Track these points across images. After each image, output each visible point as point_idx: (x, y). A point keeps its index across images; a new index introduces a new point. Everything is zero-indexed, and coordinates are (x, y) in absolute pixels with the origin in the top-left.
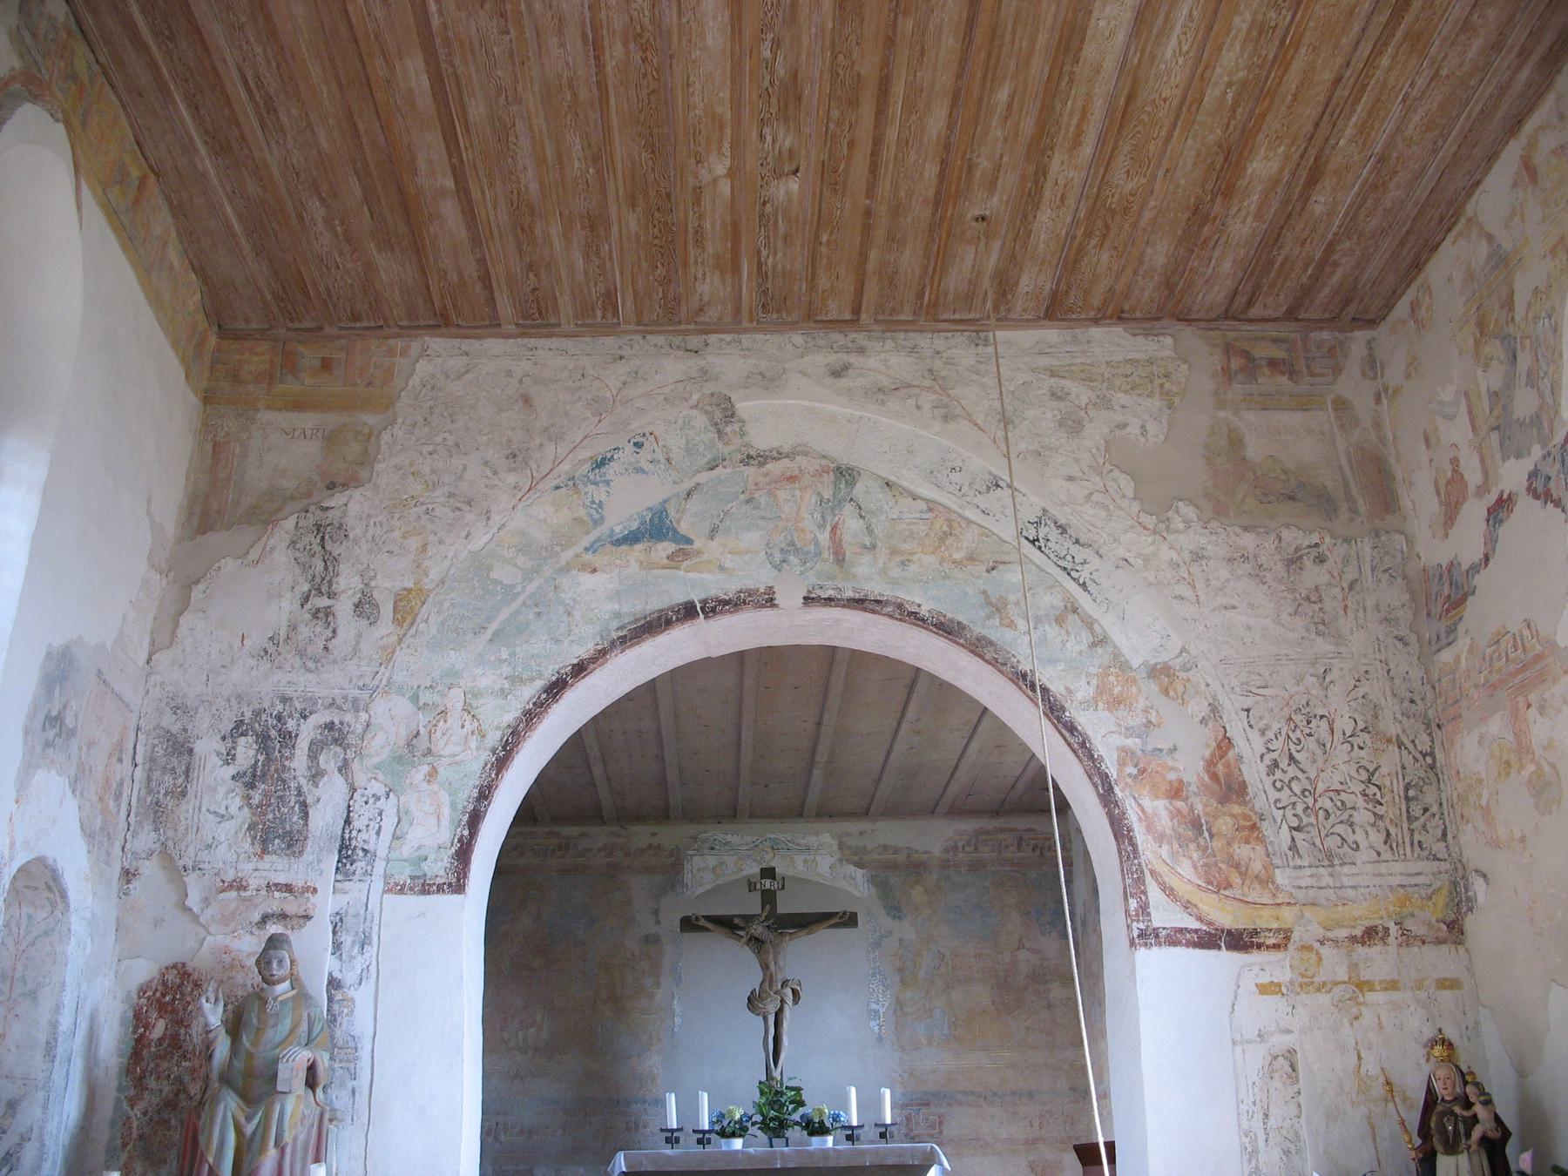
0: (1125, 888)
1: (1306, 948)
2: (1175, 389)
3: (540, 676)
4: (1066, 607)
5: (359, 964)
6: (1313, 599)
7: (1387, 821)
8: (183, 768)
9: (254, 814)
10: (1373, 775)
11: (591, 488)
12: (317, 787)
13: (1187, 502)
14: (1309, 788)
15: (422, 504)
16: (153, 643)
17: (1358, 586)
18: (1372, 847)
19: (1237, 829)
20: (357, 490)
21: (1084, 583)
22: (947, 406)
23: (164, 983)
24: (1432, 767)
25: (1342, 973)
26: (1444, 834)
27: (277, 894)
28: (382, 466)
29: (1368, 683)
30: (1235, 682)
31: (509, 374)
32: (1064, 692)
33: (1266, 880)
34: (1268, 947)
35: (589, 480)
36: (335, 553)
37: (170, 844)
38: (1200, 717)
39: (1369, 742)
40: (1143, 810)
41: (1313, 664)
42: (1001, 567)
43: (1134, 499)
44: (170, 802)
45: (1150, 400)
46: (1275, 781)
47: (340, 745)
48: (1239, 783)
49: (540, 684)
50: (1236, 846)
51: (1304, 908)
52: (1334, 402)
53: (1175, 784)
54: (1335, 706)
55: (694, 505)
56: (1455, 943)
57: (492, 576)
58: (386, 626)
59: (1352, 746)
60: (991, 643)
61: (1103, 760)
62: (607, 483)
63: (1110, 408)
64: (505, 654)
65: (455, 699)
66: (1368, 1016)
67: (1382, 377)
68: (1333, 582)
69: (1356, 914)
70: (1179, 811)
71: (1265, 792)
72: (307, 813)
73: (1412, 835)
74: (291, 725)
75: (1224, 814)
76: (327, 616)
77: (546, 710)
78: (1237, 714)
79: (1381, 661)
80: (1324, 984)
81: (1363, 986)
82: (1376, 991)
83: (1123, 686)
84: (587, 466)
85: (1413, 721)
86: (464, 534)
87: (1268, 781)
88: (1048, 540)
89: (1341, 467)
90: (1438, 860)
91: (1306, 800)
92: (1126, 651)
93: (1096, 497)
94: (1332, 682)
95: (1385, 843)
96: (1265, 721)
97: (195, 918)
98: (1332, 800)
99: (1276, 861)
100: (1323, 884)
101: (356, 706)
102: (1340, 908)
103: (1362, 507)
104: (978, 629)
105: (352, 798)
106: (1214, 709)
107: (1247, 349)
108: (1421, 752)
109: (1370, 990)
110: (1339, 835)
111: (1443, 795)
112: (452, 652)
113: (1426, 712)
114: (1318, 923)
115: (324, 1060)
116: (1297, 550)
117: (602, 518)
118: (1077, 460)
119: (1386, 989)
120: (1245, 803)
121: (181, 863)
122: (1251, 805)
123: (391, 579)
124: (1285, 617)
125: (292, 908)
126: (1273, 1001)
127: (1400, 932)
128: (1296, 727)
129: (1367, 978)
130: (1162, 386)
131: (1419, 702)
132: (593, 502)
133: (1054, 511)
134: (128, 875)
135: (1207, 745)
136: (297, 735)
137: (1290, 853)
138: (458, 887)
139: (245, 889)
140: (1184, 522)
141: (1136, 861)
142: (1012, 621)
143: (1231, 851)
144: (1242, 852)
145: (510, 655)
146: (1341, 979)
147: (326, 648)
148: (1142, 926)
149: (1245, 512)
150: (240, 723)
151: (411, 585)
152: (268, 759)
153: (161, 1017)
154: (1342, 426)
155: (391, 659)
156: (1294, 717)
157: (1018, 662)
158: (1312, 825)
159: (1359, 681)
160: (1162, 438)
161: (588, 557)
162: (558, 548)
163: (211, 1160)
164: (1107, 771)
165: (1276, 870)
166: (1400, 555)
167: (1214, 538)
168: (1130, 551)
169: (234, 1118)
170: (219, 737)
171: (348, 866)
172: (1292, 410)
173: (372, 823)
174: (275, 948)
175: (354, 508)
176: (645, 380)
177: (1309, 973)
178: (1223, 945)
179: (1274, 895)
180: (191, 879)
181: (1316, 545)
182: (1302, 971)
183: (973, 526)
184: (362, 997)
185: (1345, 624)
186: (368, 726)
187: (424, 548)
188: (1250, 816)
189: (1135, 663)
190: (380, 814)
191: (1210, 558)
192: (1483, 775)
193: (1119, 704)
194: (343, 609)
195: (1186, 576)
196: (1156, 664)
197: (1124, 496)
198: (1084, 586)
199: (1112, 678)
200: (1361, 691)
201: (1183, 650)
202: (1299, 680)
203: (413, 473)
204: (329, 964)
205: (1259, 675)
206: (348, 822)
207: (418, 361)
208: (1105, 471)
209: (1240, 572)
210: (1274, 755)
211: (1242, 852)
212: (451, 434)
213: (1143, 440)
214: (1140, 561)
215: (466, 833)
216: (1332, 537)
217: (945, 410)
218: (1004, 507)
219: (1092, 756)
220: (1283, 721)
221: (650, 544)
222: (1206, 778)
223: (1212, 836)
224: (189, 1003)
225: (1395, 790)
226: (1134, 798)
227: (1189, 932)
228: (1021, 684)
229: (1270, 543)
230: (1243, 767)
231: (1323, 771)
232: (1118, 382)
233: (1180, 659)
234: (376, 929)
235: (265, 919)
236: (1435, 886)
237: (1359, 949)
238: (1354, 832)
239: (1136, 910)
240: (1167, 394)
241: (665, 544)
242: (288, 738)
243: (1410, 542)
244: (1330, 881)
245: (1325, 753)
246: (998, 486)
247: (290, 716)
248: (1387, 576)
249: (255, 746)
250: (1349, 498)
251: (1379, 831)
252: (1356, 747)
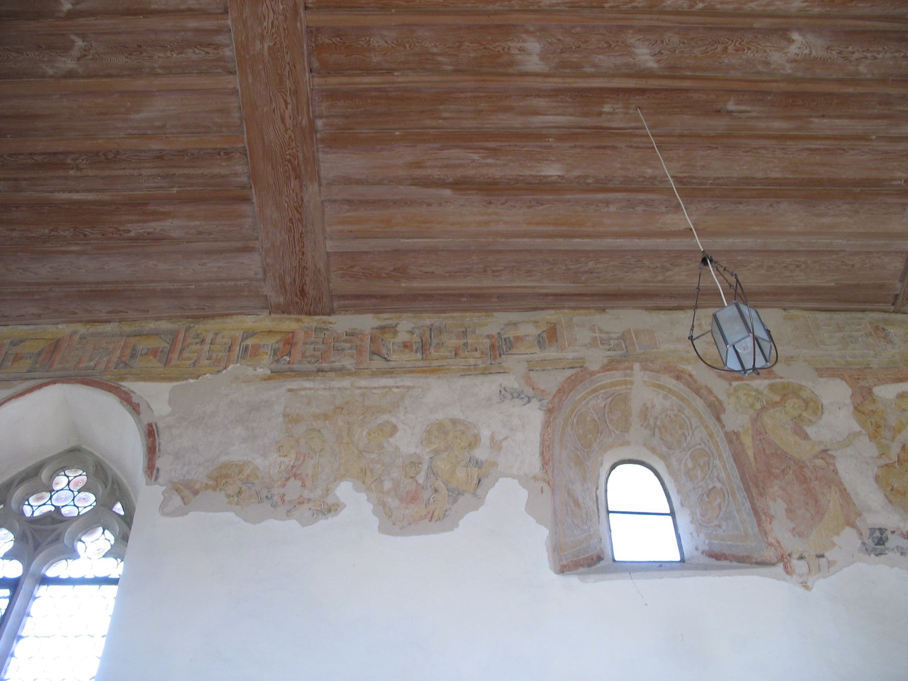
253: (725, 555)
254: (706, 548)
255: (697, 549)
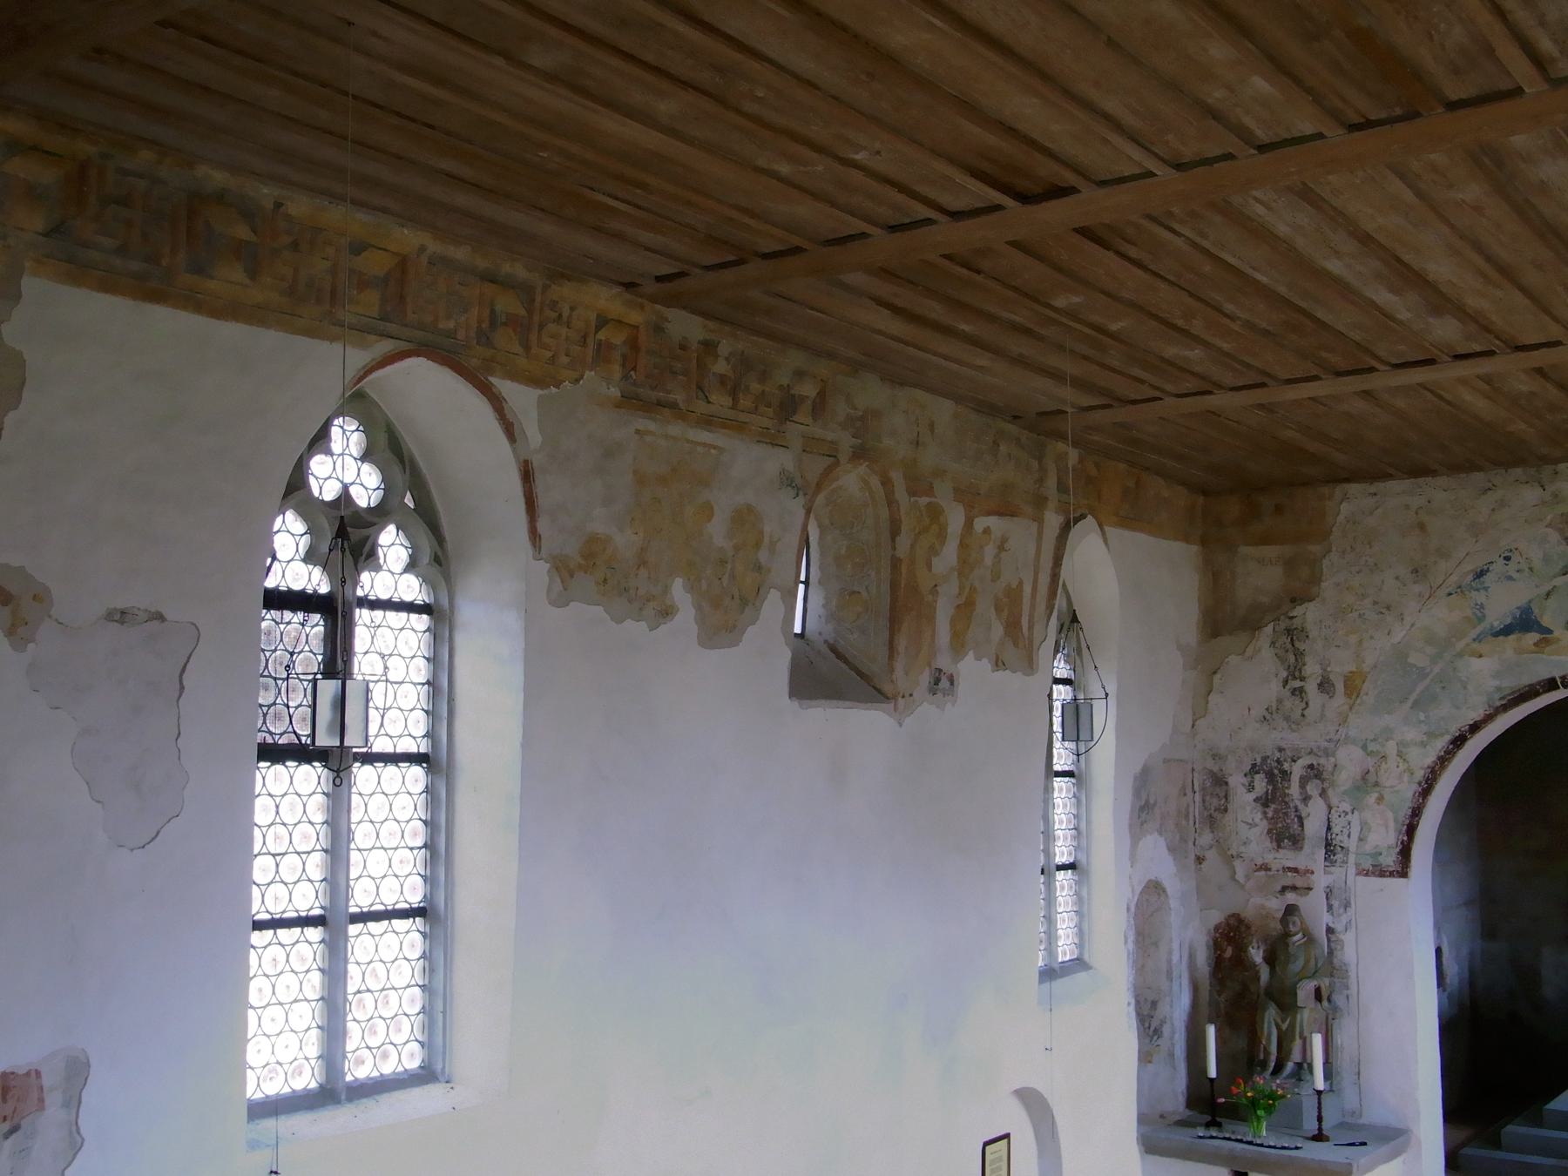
3: (1447, 732)
5: (1344, 919)
8: (1224, 794)
9: (1269, 824)
11: (1474, 593)
12: (1307, 806)
15: (1356, 610)
16: (1194, 714)
20: (1310, 603)
23: (1228, 924)
27: (1289, 874)
28: (1327, 584)
31: (1407, 507)
35: (1472, 588)
36: (1302, 648)
37: (1221, 840)
44: (1217, 815)
47: (1320, 779)
49: (1448, 738)
55: (1552, 603)
57: (1409, 660)
58: (1340, 699)
62: (1486, 589)
64: (1422, 716)
65: (1391, 748)
72: (1303, 824)
74: (1286, 766)
76: (1301, 693)
77: (1453, 756)
84: (1470, 577)
86: (1386, 632)
97: (1242, 887)
101: (1327, 753)
105: (1330, 813)
112: (1386, 716)
115: (1325, 983)
117: (1484, 616)
121: (1229, 853)
123: (1341, 665)
125: (1299, 884)
132: (1477, 604)
134: (1200, 860)
136: (1291, 773)
138: (1403, 873)
139: (1270, 870)
145: (1425, 717)
147: (1303, 715)
150: (1254, 766)
151: (1354, 669)
152: (1275, 789)
153: (1229, 945)
155: (1346, 721)
161: (1475, 645)
162: (1454, 640)
163: (1264, 1042)
169: (1275, 1020)
170: (1242, 775)
171: (1332, 857)
173: (1345, 830)
174: (1290, 915)
175: (1310, 617)
176: (1509, 506)
180: (1237, 863)
184: (1348, 938)
186: (1336, 766)
187: (1360, 642)
190: (1349, 824)
194: (1311, 687)
203: (1347, 589)
204: (1326, 919)
206: (1329, 828)
207: (1341, 503)
212: (1371, 557)
215: (1405, 838)
221: (1519, 635)
224: (1244, 938)
234: (1352, 897)
235: (1284, 889)
241: (1533, 634)
242: (1286, 775)
247: (1285, 760)
249: (1266, 780)
253: (846, 658)
254: (831, 641)
255: (820, 634)
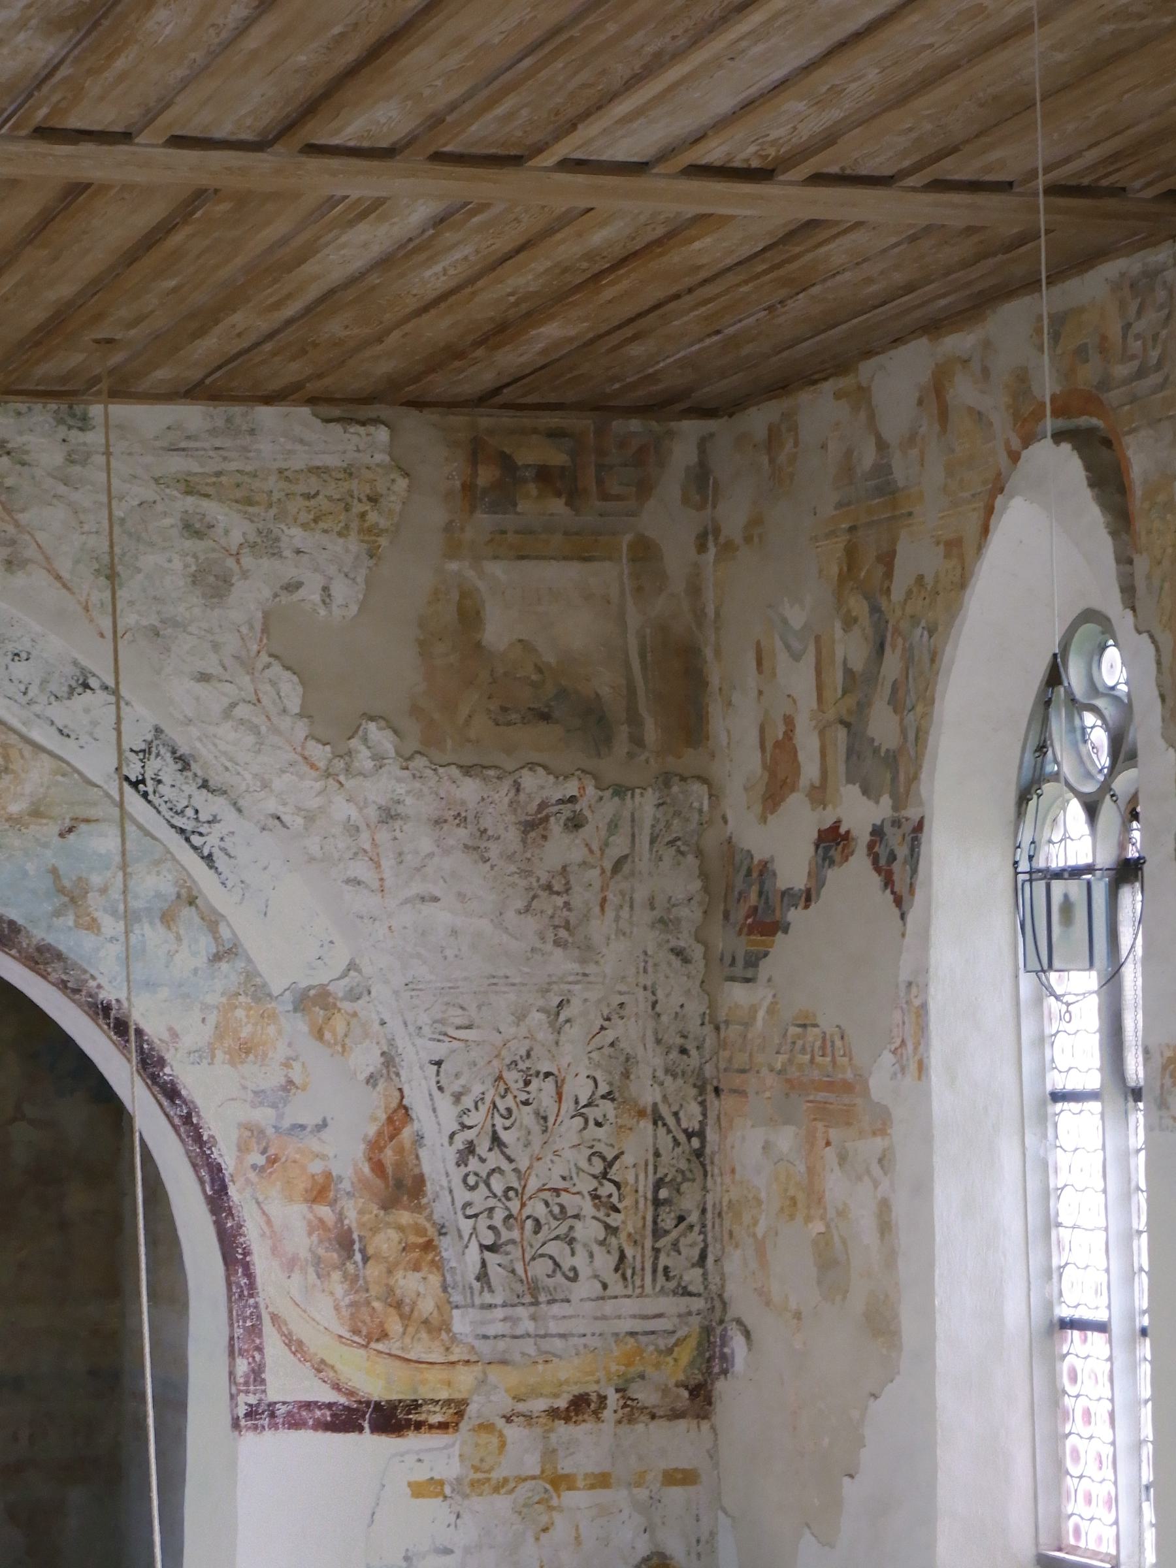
0: (232, 1338)
1: (486, 1427)
2: (383, 523)
4: (179, 896)
6: (556, 888)
7: (623, 1236)
10: (610, 1165)
13: (383, 723)
14: (516, 1185)
17: (626, 868)
18: (596, 1277)
19: (404, 1249)
21: (210, 855)
22: (13, 542)
24: (699, 1153)
25: (532, 1464)
26: (703, 1256)
29: (621, 1022)
30: (424, 1019)
32: (166, 1036)
33: (437, 1327)
34: (431, 1427)
38: (366, 1074)
39: (611, 1114)
40: (269, 1222)
41: (545, 991)
42: (83, 827)
43: (301, 715)
45: (341, 541)
46: (467, 1175)
48: (415, 1176)
50: (399, 1274)
51: (490, 1368)
52: (632, 547)
53: (321, 1180)
54: (568, 1059)
56: (698, 1416)
59: (586, 1121)
60: (59, 956)
61: (215, 1144)
63: (277, 554)
66: (562, 1529)
67: (714, 507)
68: (590, 859)
69: (563, 1376)
70: (321, 1221)
71: (451, 1191)
73: (656, 1258)
75: (388, 1225)
78: (421, 1068)
79: (645, 988)
80: (506, 1481)
81: (560, 1482)
82: (579, 1489)
83: (256, 1024)
85: (680, 1081)
87: (457, 1174)
88: (159, 782)
89: (628, 665)
90: (690, 1294)
91: (508, 1204)
92: (262, 968)
93: (242, 711)
94: (568, 1021)
95: (616, 1270)
96: (462, 1081)
98: (547, 1204)
99: (456, 1298)
100: (519, 1332)
102: (540, 1367)
103: (651, 733)
104: (39, 934)
106: (389, 1060)
107: (507, 450)
108: (685, 1131)
109: (569, 1489)
110: (551, 1257)
111: (710, 1198)
113: (701, 1069)
114: (507, 1391)
116: (543, 805)
118: (216, 647)
119: (592, 1487)
120: (419, 1208)
122: (428, 1210)
124: (510, 915)
126: (432, 1506)
127: (621, 1402)
128: (507, 1090)
129: (566, 1472)
130: (363, 515)
131: (693, 1052)
133: (174, 733)
135: (374, 1119)
137: (477, 1285)
140: (373, 759)
141: (251, 1301)
142: (94, 920)
143: (392, 1282)
144: (408, 1283)
146: (531, 1473)
148: (252, 1399)
149: (469, 741)
154: (639, 589)
156: (506, 1075)
157: (99, 987)
158: (513, 1242)
159: (608, 1019)
160: (354, 608)
164: (220, 1160)
165: (455, 1312)
166: (695, 817)
167: (417, 785)
168: (285, 804)
172: (565, 558)
177: (486, 1466)
178: (366, 1425)
179: (447, 1349)
181: (572, 799)
182: (476, 1462)
183: (44, 756)
185: (599, 928)
188: (426, 1230)
189: (276, 990)
191: (405, 818)
192: (763, 1195)
193: (247, 1053)
195: (367, 846)
196: (310, 988)
197: (284, 711)
198: (209, 859)
199: (240, 1013)
200: (610, 1036)
201: (352, 966)
202: (520, 1017)
205: (462, 1008)
208: (259, 666)
209: (451, 842)
210: (470, 1135)
211: (408, 1283)
213: (323, 612)
214: (300, 821)
216: (597, 788)
217: (9, 550)
218: (94, 723)
219: (200, 1136)
220: (489, 1081)
222: (366, 1169)
223: (366, 1259)
225: (641, 1189)
226: (258, 1203)
227: (320, 1408)
228: (101, 1021)
229: (502, 794)
230: (423, 1153)
231: (539, 1159)
232: (293, 507)
233: (347, 980)
236: (679, 1334)
237: (563, 1430)
238: (573, 1254)
239: (247, 1376)
240: (369, 531)
243: (714, 796)
244: (528, 1326)
245: (545, 1131)
246: (86, 686)
248: (672, 851)
250: (634, 719)
251: (609, 1252)
252: (591, 1123)
